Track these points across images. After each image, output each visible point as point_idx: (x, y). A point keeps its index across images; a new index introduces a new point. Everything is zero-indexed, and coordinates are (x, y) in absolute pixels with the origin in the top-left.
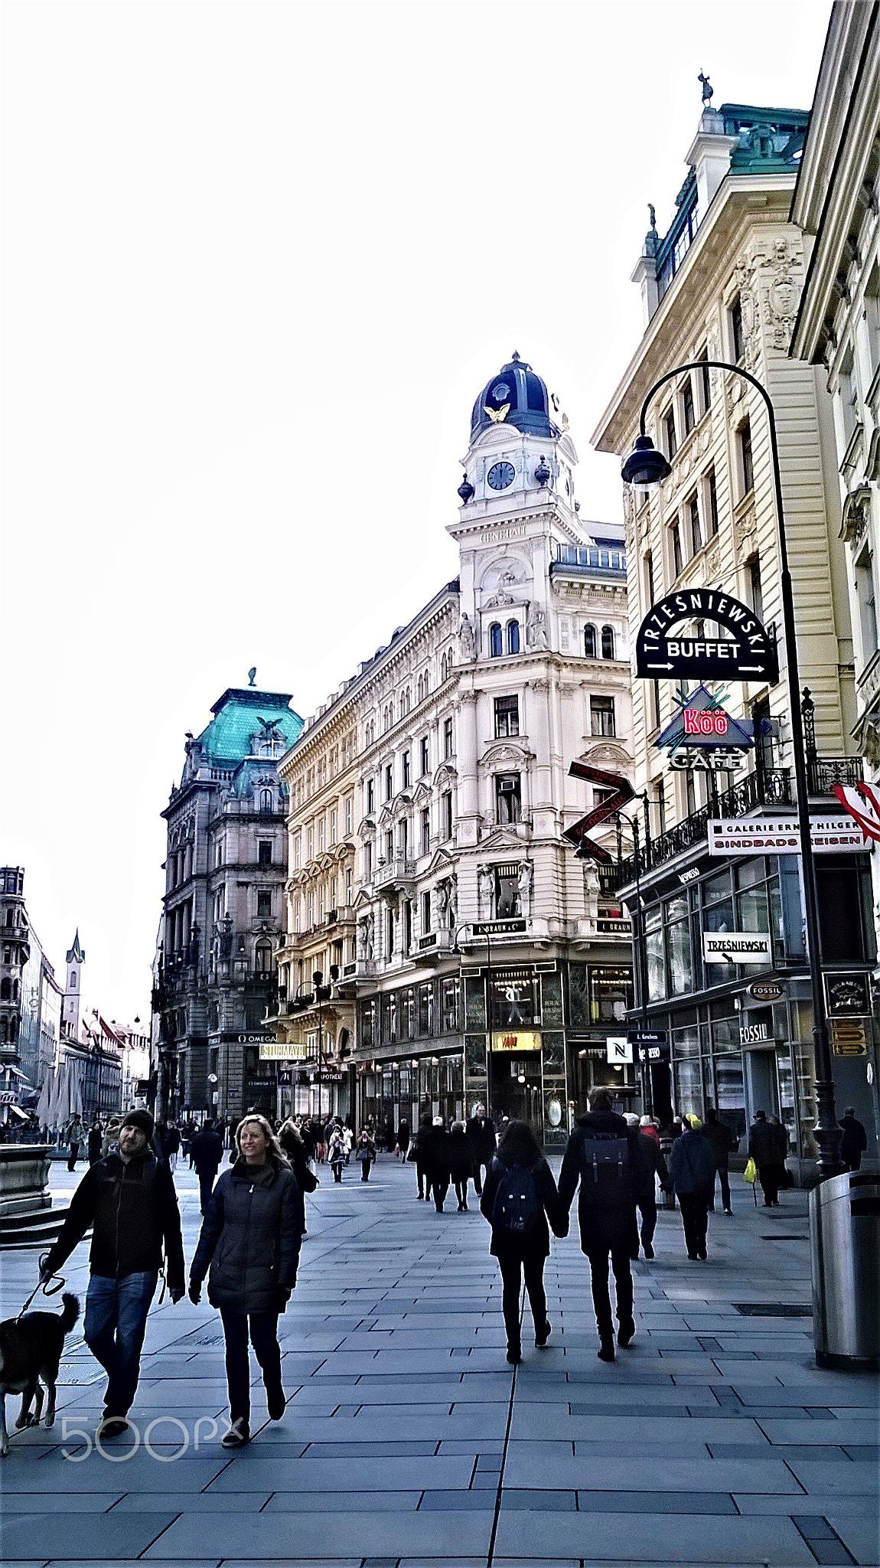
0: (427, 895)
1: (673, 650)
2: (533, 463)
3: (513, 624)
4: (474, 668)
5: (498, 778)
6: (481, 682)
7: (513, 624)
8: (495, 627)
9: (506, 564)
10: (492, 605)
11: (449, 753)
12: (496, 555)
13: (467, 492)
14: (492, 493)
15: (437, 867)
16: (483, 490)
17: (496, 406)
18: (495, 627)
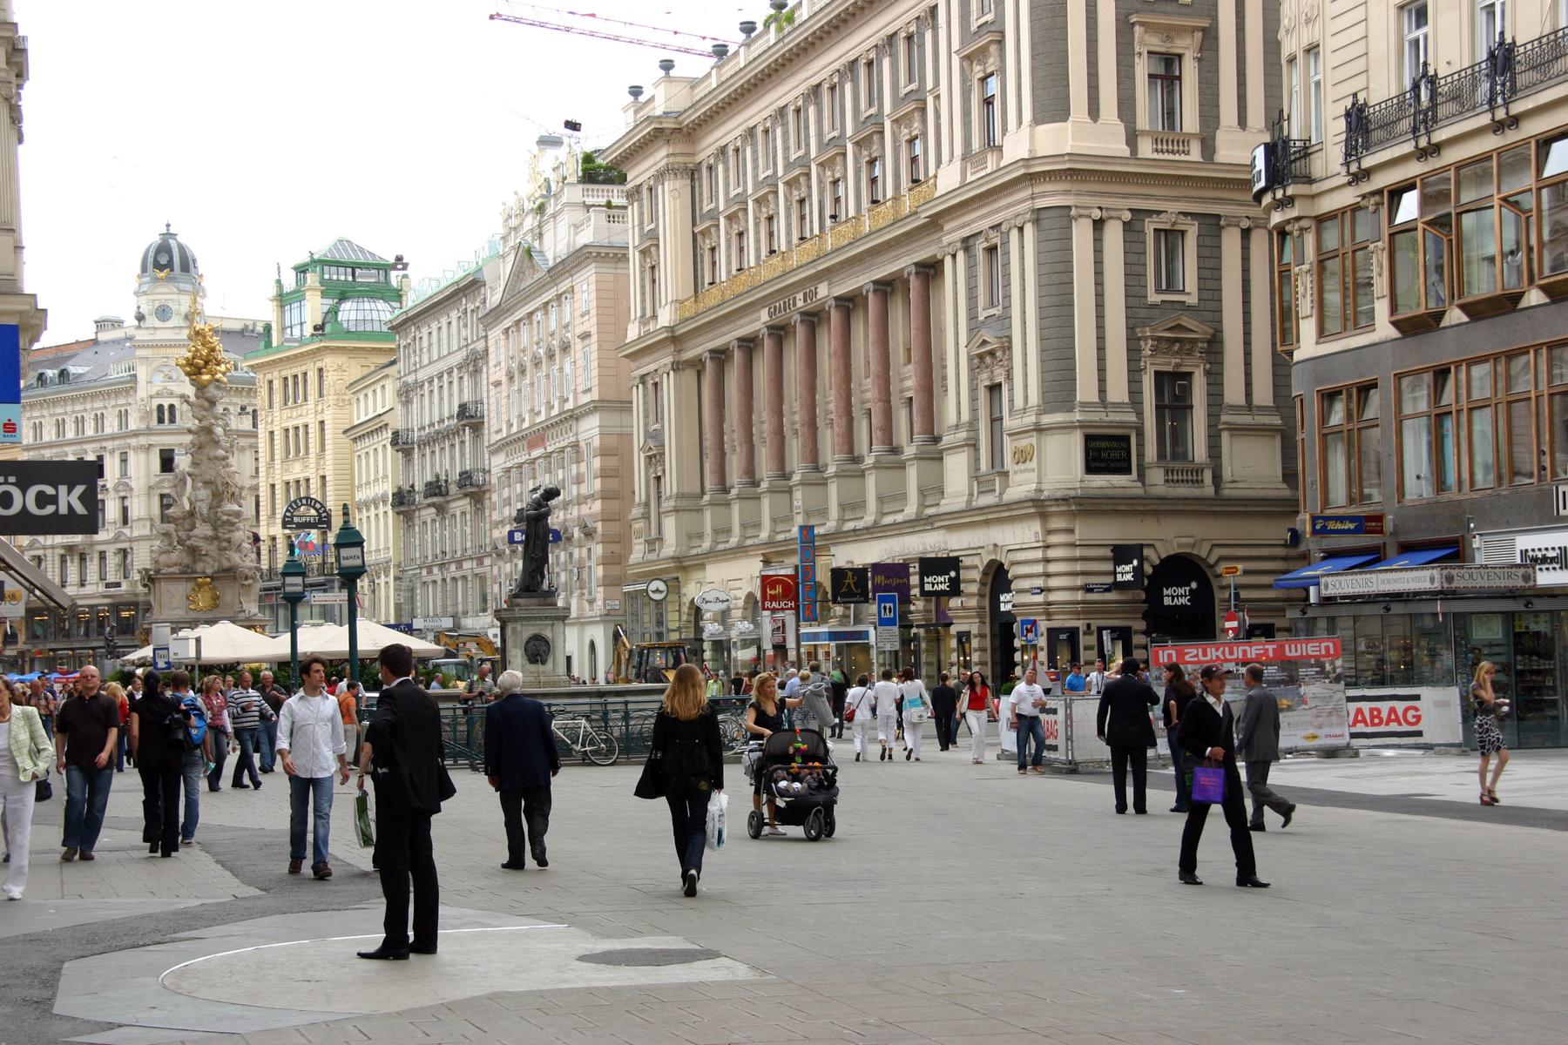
0: (102, 556)
1: (296, 520)
2: (184, 309)
3: (172, 407)
4: (149, 432)
5: (162, 496)
6: (153, 440)
7: (172, 407)
8: (160, 408)
9: (166, 370)
10: (158, 395)
11: (124, 474)
12: (160, 362)
13: (140, 318)
14: (158, 324)
15: (116, 539)
16: (151, 321)
17: (159, 266)
18: (160, 408)
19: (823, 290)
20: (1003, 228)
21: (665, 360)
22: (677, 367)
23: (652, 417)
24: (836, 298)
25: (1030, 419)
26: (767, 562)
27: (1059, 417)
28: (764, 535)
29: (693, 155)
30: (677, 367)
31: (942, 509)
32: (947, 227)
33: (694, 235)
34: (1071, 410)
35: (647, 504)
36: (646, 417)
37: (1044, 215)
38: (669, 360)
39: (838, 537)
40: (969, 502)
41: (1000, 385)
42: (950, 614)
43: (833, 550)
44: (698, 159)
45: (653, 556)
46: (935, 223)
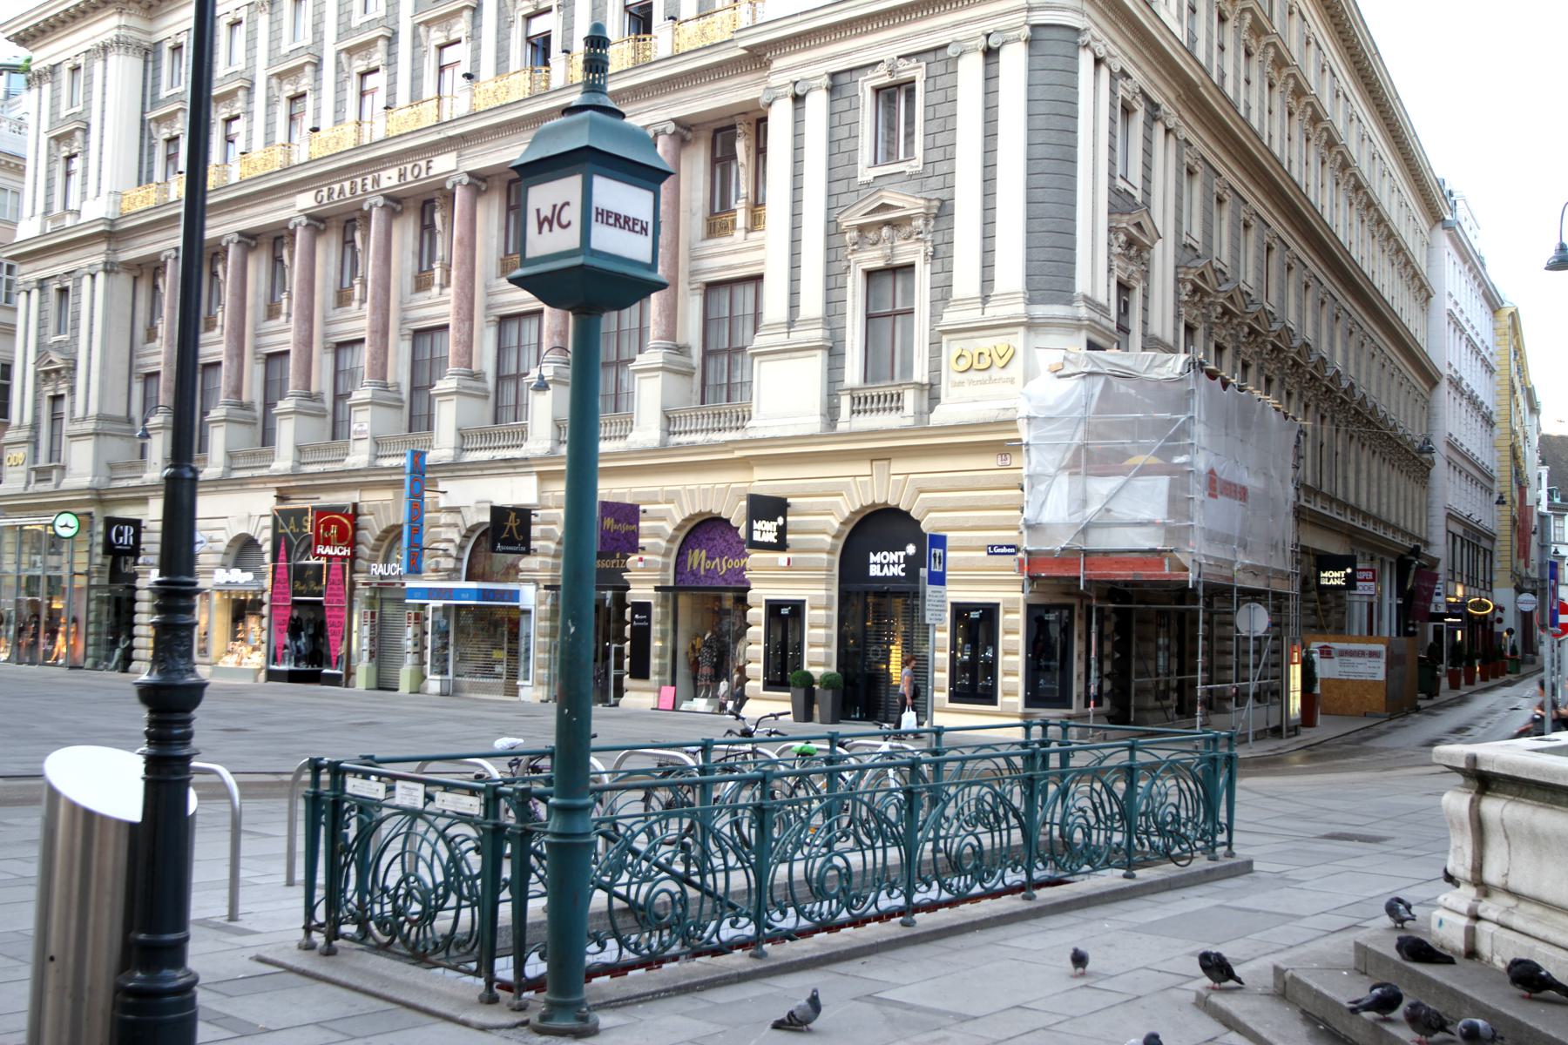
19: (444, 164)
20: (950, 52)
21: (95, 257)
22: (110, 269)
23: (52, 326)
24: (470, 174)
25: (1018, 309)
26: (281, 498)
27: (1058, 310)
28: (283, 462)
29: (150, 33)
30: (110, 269)
31: (751, 434)
32: (778, 64)
33: (143, 121)
34: (1069, 302)
35: (35, 426)
36: (42, 324)
37: (1044, 34)
38: (102, 258)
39: (455, 469)
40: (457, 456)
41: (910, 267)
42: (626, 576)
43: (442, 486)
44: (157, 38)
45: (41, 487)
46: (757, 58)
